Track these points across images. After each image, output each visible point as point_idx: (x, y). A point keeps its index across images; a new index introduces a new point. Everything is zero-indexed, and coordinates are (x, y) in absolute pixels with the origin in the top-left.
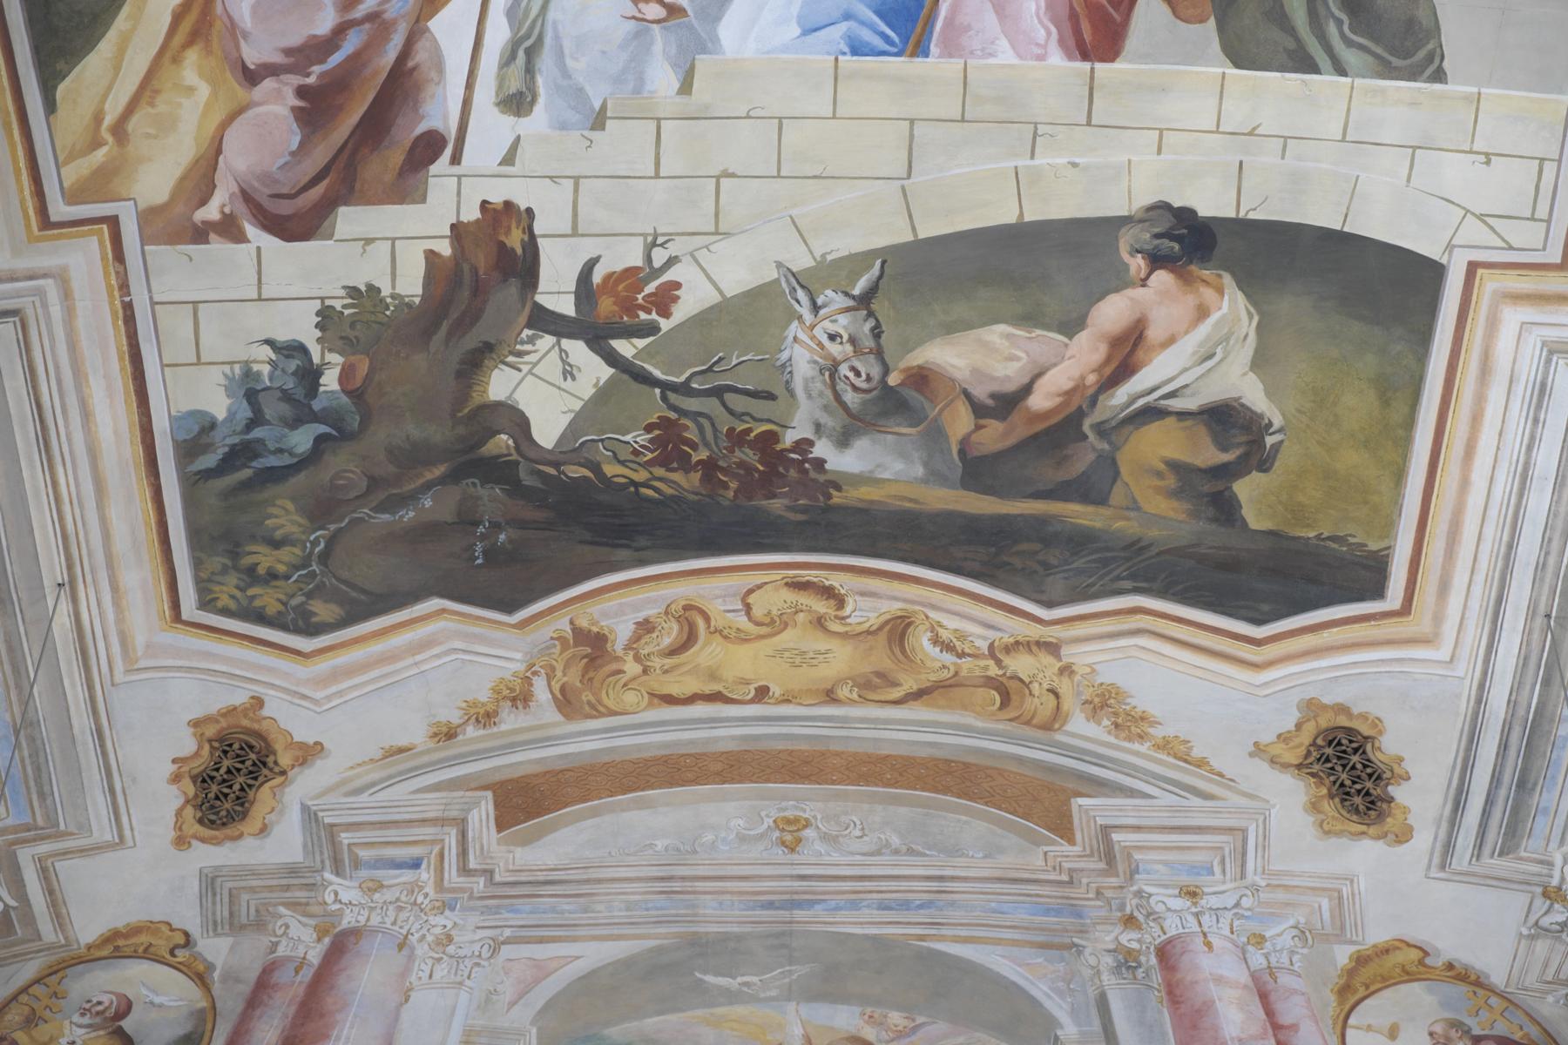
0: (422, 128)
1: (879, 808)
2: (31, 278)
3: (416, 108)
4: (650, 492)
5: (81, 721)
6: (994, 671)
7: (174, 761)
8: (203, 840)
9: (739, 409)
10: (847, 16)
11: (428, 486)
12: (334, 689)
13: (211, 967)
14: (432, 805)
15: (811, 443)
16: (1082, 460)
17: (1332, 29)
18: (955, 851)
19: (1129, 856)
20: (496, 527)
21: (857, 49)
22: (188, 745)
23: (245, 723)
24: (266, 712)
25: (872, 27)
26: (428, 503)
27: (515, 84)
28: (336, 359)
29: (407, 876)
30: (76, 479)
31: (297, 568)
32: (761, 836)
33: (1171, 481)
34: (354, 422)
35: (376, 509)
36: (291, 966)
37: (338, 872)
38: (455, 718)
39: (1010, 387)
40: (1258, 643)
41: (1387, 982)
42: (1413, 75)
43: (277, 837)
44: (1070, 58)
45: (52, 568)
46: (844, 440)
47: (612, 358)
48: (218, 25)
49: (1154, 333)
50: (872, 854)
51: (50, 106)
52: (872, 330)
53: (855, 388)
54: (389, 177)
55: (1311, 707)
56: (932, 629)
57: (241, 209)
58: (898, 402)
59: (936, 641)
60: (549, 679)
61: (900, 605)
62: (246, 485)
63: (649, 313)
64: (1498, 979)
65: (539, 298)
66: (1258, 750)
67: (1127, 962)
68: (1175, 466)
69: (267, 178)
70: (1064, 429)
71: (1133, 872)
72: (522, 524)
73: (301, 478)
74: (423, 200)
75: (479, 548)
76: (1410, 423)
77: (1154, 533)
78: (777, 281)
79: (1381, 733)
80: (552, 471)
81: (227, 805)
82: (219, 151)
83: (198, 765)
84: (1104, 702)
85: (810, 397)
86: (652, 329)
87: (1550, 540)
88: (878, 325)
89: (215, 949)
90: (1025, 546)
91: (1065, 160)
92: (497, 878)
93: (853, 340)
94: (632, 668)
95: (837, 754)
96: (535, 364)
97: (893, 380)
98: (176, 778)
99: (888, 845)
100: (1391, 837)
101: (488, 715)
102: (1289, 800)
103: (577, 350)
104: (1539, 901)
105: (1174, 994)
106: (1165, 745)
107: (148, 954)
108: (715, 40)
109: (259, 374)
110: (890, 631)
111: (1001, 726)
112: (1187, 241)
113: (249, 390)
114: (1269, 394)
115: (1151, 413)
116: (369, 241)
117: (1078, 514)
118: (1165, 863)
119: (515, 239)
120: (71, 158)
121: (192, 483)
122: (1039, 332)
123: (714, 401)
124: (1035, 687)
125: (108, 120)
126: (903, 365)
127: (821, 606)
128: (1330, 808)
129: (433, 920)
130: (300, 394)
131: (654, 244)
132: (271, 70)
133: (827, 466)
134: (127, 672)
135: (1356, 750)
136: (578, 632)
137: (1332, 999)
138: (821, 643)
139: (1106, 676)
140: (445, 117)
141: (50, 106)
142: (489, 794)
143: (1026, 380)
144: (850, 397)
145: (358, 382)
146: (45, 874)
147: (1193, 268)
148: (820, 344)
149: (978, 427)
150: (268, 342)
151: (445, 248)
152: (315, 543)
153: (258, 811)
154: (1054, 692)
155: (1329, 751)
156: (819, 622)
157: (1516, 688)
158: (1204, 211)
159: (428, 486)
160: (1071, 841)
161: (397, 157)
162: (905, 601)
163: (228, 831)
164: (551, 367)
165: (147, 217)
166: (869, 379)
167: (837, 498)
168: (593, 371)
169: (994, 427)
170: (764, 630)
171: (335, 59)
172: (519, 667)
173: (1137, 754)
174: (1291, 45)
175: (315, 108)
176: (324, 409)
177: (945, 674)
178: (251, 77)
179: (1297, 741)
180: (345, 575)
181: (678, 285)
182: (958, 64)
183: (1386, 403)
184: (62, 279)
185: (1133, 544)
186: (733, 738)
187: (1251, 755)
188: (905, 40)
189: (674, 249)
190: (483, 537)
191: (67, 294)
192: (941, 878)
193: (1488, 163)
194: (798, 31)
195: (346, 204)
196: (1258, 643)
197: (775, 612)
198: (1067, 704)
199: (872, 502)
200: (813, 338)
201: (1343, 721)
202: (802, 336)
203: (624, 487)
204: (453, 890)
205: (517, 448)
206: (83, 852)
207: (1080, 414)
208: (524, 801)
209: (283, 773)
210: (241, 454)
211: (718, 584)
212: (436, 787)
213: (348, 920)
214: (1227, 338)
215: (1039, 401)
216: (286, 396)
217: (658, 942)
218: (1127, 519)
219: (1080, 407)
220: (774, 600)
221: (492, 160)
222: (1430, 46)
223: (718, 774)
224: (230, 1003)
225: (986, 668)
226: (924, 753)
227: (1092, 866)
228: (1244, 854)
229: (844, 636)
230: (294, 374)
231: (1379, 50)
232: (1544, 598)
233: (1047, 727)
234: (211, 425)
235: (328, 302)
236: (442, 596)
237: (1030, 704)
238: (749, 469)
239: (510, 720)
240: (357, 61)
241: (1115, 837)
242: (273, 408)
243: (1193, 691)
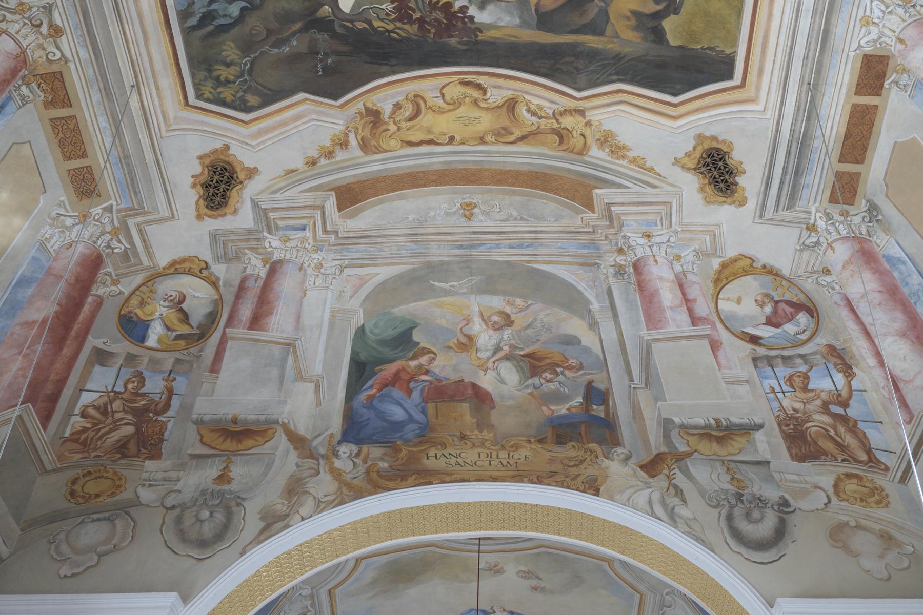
1: (507, 197)
4: (395, 35)
5: (149, 156)
6: (556, 125)
7: (193, 177)
8: (209, 216)
11: (294, 34)
12: (260, 140)
13: (218, 279)
14: (309, 199)
15: (467, 8)
18: (541, 218)
19: (619, 218)
20: (326, 55)
22: (198, 169)
23: (222, 157)
24: (231, 152)
26: (295, 43)
29: (300, 234)
30: (134, 30)
31: (239, 77)
32: (455, 213)
33: (633, 22)
36: (253, 279)
37: (270, 233)
38: (315, 154)
40: (675, 105)
41: (736, 276)
43: (240, 217)
45: (129, 79)
50: (505, 221)
55: (700, 138)
59: (529, 111)
61: (512, 92)
62: (211, 34)
64: (786, 272)
66: (676, 162)
67: (620, 271)
68: (635, 14)
71: (622, 226)
72: (338, 53)
73: (235, 31)
75: (319, 66)
77: (626, 50)
79: (732, 150)
80: (349, 25)
81: (218, 199)
83: (204, 179)
84: (606, 140)
89: (219, 270)
90: (567, 59)
92: (340, 235)
94: (393, 128)
95: (487, 170)
98: (194, 186)
99: (511, 216)
100: (737, 203)
101: (330, 153)
102: (690, 186)
104: (804, 232)
105: (641, 286)
106: (634, 161)
107: (190, 272)
110: (508, 106)
111: (560, 154)
117: (591, 41)
118: (635, 221)
121: (187, 32)
127: (476, 94)
128: (708, 189)
129: (314, 256)
134: (168, 131)
135: (721, 159)
136: (367, 109)
137: (712, 285)
138: (477, 113)
139: (606, 126)
142: (333, 193)
146: (141, 232)
153: (232, 202)
154: (583, 135)
155: (708, 160)
156: (475, 102)
157: (794, 123)
159: (294, 34)
160: (593, 212)
162: (514, 90)
163: (219, 212)
167: (481, 37)
170: (451, 107)
172: (342, 128)
173: (621, 166)
177: (534, 128)
179: (694, 156)
185: (617, 56)
186: (440, 163)
187: (673, 164)
190: (321, 61)
192: (536, 232)
196: (675, 105)
198: (588, 142)
199: (496, 38)
201: (715, 145)
203: (383, 33)
204: (321, 241)
205: (333, 13)
206: (156, 221)
208: (350, 196)
209: (241, 183)
211: (431, 83)
212: (310, 190)
213: (277, 256)
217: (412, 266)
218: (614, 43)
220: (454, 91)
223: (435, 181)
224: (229, 298)
226: (526, 168)
227: (603, 224)
228: (671, 215)
229: (487, 109)
232: (807, 75)
233: (580, 153)
237: (573, 142)
238: (440, 22)
239: (340, 155)
241: (613, 208)
243: (644, 129)
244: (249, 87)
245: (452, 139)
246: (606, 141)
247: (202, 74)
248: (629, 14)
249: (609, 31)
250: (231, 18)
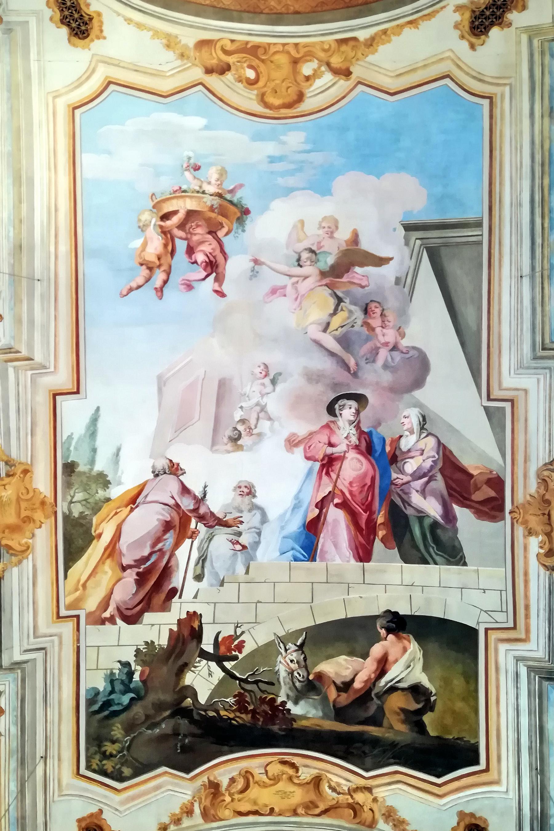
0: (170, 587)
2: (51, 636)
3: (170, 580)
9: (263, 689)
10: (293, 549)
11: (164, 719)
16: (372, 709)
17: (431, 550)
20: (185, 736)
21: (296, 559)
23: (96, 821)
24: (104, 816)
25: (300, 552)
27: (199, 571)
28: (139, 668)
31: (119, 752)
33: (402, 716)
34: (143, 693)
35: (147, 729)
39: (348, 679)
40: (439, 786)
42: (457, 564)
44: (357, 561)
45: (40, 751)
46: (296, 703)
47: (224, 669)
48: (117, 551)
49: (391, 658)
51: (66, 577)
52: (304, 658)
53: (299, 681)
54: (161, 602)
55: (462, 815)
56: (328, 782)
57: (116, 613)
58: (312, 687)
59: (330, 787)
60: (200, 803)
61: (317, 771)
62: (107, 718)
63: (235, 652)
65: (202, 646)
68: (403, 710)
69: (125, 602)
70: (365, 697)
72: (194, 735)
73: (123, 716)
74: (170, 611)
76: (476, 691)
77: (398, 738)
78: (274, 640)
80: (203, 713)
82: (112, 593)
85: (285, 684)
86: (235, 658)
87: (531, 736)
88: (305, 655)
90: (357, 745)
91: (358, 596)
93: (298, 662)
94: (228, 799)
96: (200, 671)
97: (311, 677)
103: (213, 665)
108: (256, 556)
109: (115, 673)
112: (398, 623)
113: (111, 680)
114: (430, 680)
115: (393, 689)
116: (153, 625)
119: (196, 625)
120: (70, 594)
121: (90, 715)
122: (355, 658)
123: (255, 686)
124: (365, 808)
125: (82, 582)
126: (314, 671)
127: (291, 772)
130: (127, 682)
131: (237, 627)
132: (130, 567)
133: (291, 712)
138: (291, 788)
139: (389, 803)
140: (178, 583)
141: (66, 577)
143: (352, 677)
144: (298, 684)
145: (145, 678)
147: (401, 633)
148: (288, 664)
149: (339, 696)
150: (119, 662)
151: (175, 628)
152: (126, 742)
154: (371, 810)
156: (290, 779)
158: (401, 613)
159: (164, 719)
161: (163, 596)
162: (319, 769)
164: (205, 672)
165: (89, 615)
166: (303, 677)
167: (295, 725)
168: (219, 674)
169: (344, 695)
170: (272, 782)
171: (149, 563)
172: (190, 798)
174: (420, 556)
175: (141, 579)
176: (133, 688)
177: (334, 802)
178: (124, 569)
180: (135, 756)
181: (244, 642)
182: (324, 564)
183: (468, 682)
184: (60, 636)
188: (309, 556)
189: (243, 628)
190: (181, 740)
191: (61, 643)
193: (484, 592)
194: (279, 554)
195: (147, 612)
196: (439, 786)
197: (276, 774)
198: (378, 815)
200: (286, 661)
201: (474, 821)
202: (282, 661)
205: (193, 703)
207: (370, 690)
210: (107, 704)
211: (257, 761)
214: (413, 659)
215: (357, 685)
216: (122, 682)
219: (370, 687)
220: (276, 769)
221: (192, 596)
222: (461, 554)
225: (347, 799)
230: (126, 674)
231: (446, 556)
234: (97, 693)
235: (139, 647)
236: (166, 766)
240: (154, 564)
242: (119, 687)
244: (127, 760)
245: (272, 810)
246: (390, 816)
247: (94, 749)
248: (398, 711)
249: (385, 723)
250: (122, 705)
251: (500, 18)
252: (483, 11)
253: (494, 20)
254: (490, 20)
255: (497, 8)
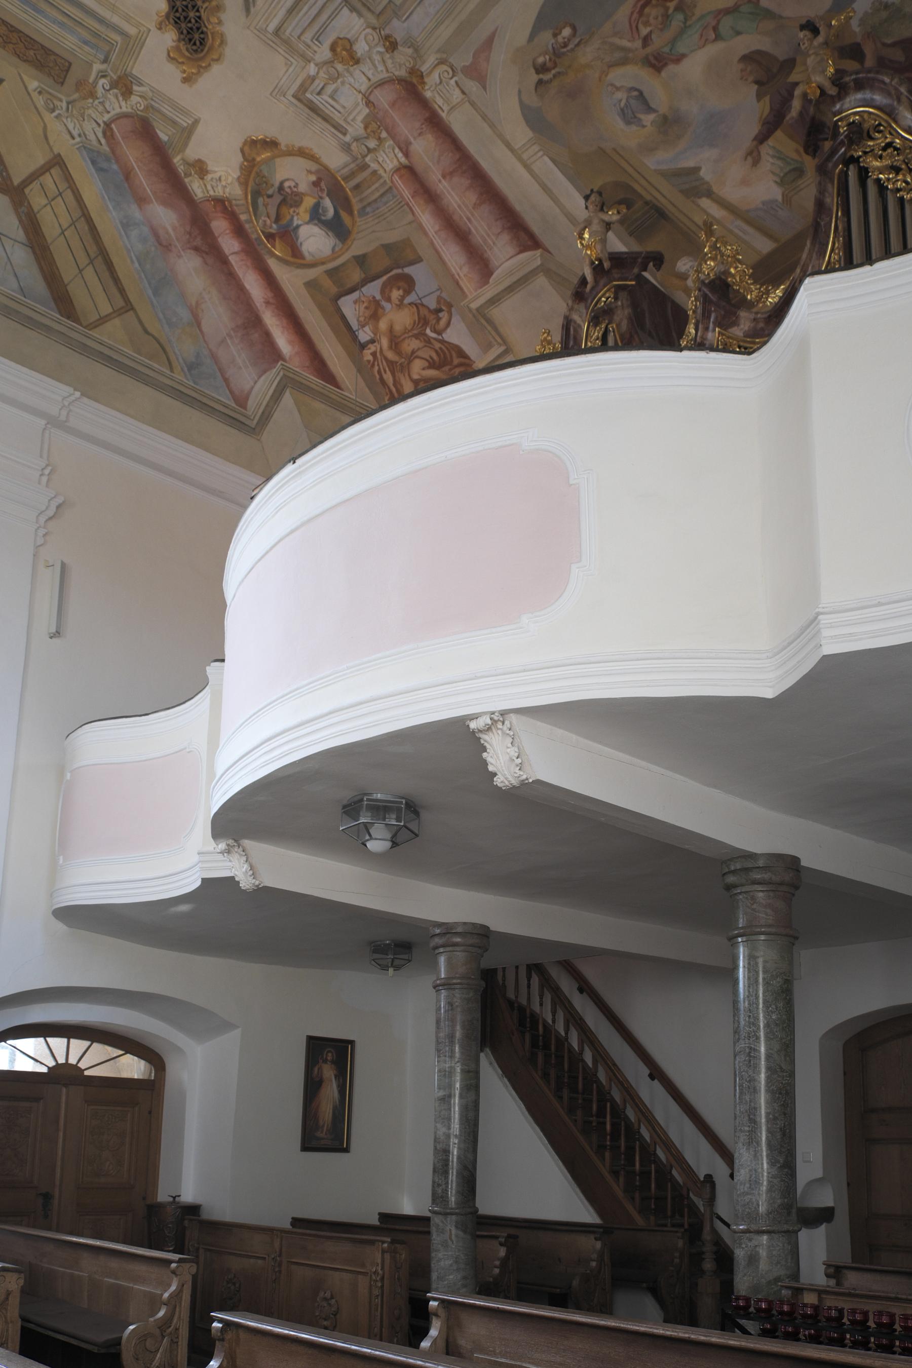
251: (176, 22)
252: (198, 11)
253: (178, 15)
254: (180, 10)
255: (191, 29)
